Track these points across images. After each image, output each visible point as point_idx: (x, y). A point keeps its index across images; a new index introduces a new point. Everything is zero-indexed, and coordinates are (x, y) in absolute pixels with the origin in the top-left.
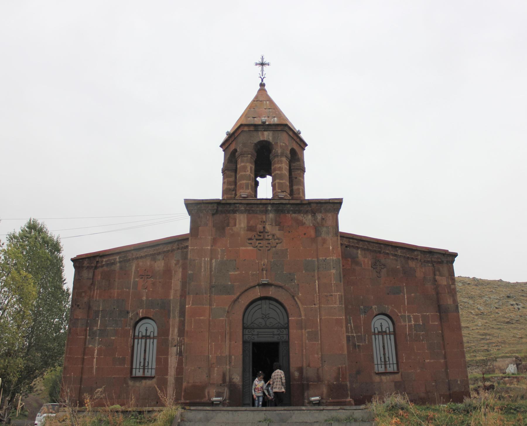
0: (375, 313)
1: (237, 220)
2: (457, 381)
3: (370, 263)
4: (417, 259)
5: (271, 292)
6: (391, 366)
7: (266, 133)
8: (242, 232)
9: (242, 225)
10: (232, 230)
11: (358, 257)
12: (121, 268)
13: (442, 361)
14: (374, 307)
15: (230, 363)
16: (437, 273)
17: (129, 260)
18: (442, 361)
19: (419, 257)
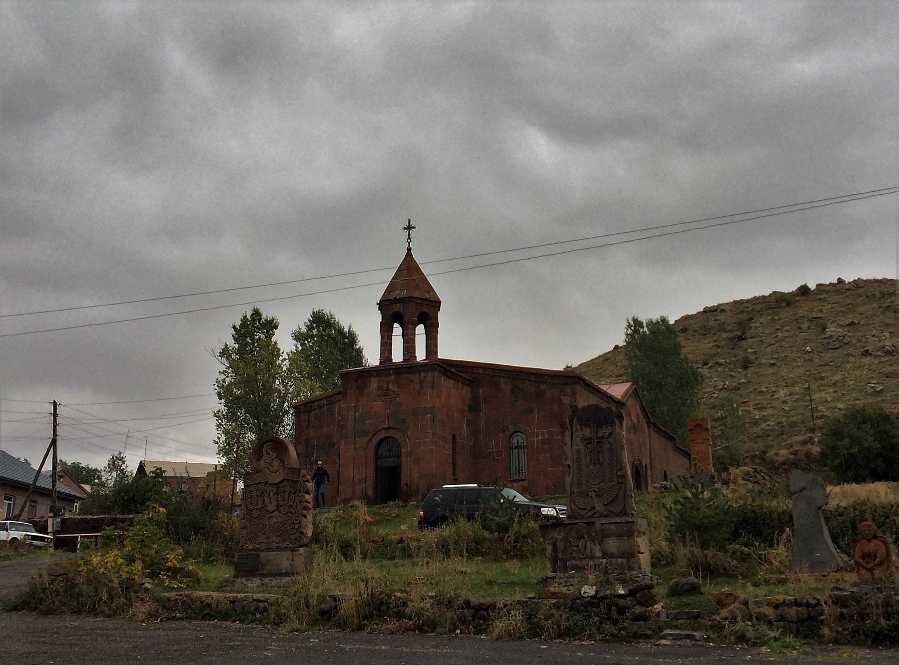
0: (511, 431)
4: (547, 382)
5: (391, 433)
6: (524, 474)
7: (398, 305)
11: (500, 385)
13: (561, 469)
14: (510, 426)
15: (366, 482)
17: (333, 403)
19: (549, 381)
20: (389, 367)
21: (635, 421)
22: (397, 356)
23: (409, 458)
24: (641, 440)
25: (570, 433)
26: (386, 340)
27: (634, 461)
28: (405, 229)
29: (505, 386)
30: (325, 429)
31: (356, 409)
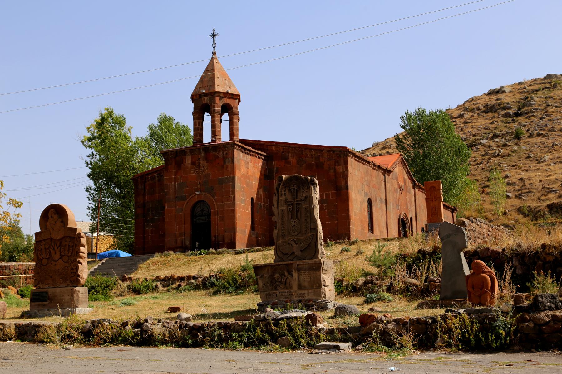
1: (187, 159)
2: (343, 235)
3: (296, 162)
7: (206, 98)
8: (189, 166)
9: (189, 162)
10: (184, 165)
11: (289, 159)
12: (159, 180)
13: (336, 222)
16: (337, 164)
18: (336, 222)
20: (200, 147)
21: (402, 184)
22: (207, 138)
23: (216, 217)
24: (407, 198)
25: (277, 197)
26: (197, 126)
27: (400, 215)
28: (210, 36)
29: (293, 160)
30: (157, 195)
31: (176, 180)
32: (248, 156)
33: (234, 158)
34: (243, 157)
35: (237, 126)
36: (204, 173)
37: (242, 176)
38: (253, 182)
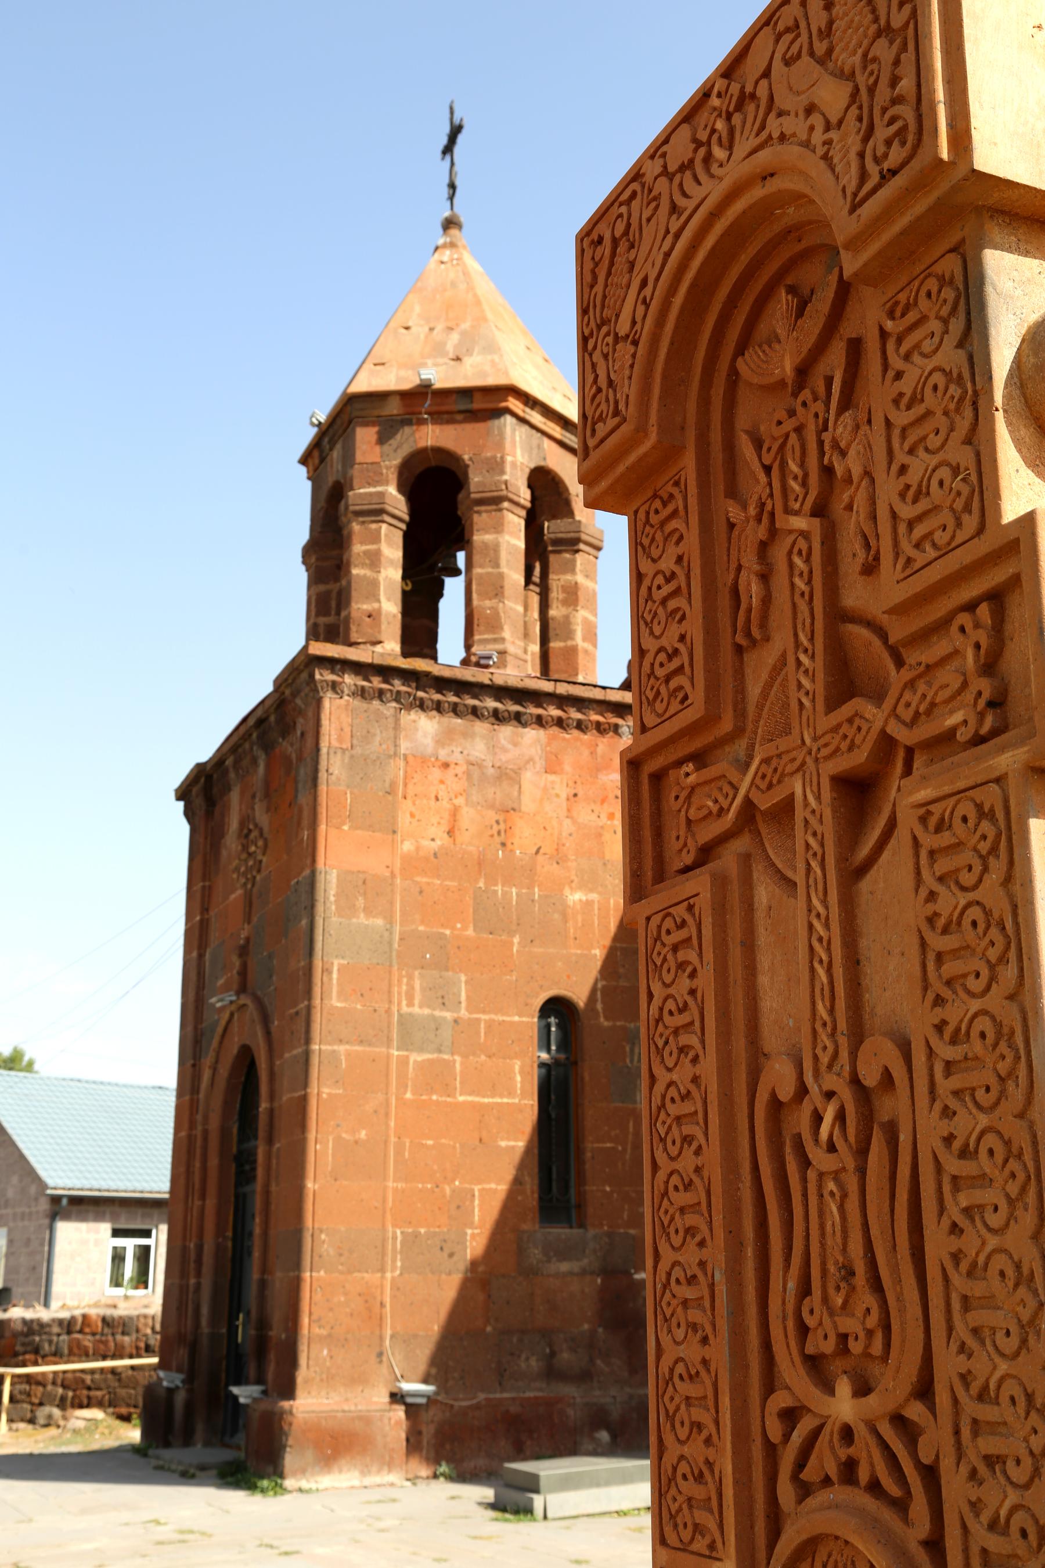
26: (312, 621)
32: (506, 732)
33: (317, 749)
34: (439, 742)
35: (497, 565)
36: (258, 878)
37: (412, 864)
38: (575, 897)
